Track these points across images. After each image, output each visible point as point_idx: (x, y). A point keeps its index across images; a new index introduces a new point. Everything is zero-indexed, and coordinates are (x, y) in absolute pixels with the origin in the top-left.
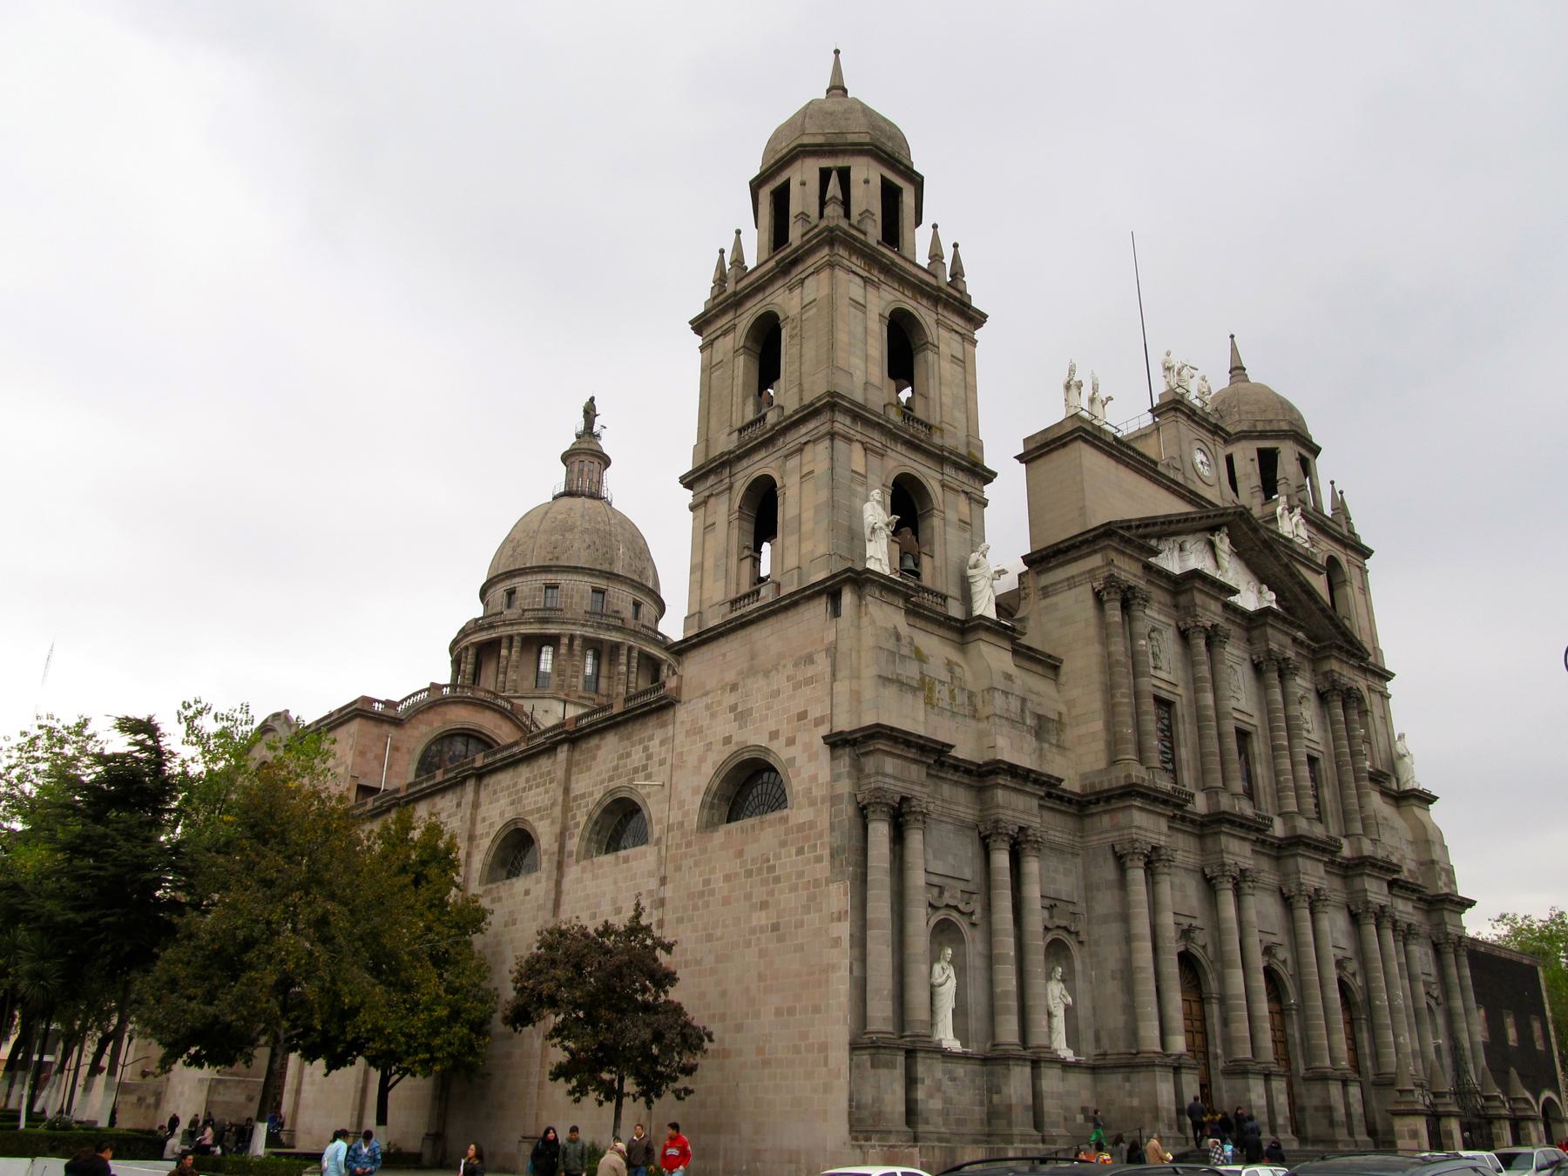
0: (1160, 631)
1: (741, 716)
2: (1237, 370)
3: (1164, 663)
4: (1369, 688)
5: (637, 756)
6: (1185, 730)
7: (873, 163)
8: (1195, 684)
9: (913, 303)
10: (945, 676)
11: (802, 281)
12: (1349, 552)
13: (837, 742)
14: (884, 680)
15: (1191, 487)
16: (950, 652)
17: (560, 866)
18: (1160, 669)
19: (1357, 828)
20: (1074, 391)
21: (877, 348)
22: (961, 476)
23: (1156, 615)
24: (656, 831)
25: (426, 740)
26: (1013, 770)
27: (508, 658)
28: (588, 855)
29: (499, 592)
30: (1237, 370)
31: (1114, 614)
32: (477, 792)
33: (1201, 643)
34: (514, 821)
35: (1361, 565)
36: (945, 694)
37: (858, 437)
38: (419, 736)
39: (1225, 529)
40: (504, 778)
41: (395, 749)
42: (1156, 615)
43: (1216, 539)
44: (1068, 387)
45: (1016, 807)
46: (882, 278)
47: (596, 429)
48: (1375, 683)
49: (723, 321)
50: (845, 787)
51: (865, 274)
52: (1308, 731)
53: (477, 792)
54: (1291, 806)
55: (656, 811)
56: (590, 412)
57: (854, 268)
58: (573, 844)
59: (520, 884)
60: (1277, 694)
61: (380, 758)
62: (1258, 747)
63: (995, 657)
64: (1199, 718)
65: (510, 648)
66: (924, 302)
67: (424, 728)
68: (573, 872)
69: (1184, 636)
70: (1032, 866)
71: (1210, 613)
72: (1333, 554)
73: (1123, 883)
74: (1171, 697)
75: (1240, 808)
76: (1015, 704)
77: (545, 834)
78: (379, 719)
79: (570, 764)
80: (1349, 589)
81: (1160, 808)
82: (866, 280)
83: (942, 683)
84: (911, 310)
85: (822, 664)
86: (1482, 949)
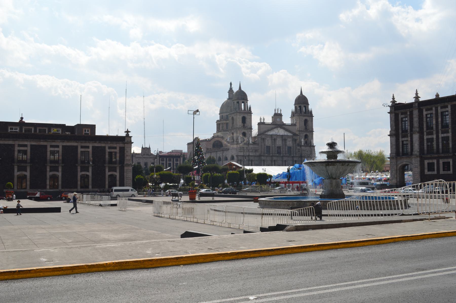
1: (232, 152)
2: (301, 92)
4: (309, 134)
5: (227, 154)
6: (271, 148)
7: (241, 101)
8: (272, 144)
11: (234, 116)
13: (236, 156)
14: (239, 151)
15: (276, 124)
16: (247, 146)
17: (223, 161)
19: (294, 153)
21: (241, 121)
23: (268, 139)
24: (228, 160)
25: (213, 143)
26: (250, 156)
27: (222, 126)
28: (224, 161)
29: (221, 115)
30: (301, 92)
31: (262, 141)
32: (217, 153)
33: (273, 141)
34: (219, 156)
38: (212, 142)
40: (218, 152)
41: (210, 144)
42: (268, 139)
44: (260, 119)
45: (251, 158)
47: (232, 88)
48: (311, 133)
49: (230, 115)
50: (237, 159)
53: (217, 153)
54: (284, 153)
55: (228, 158)
56: (231, 84)
58: (223, 159)
59: (220, 162)
60: (284, 143)
61: (208, 145)
62: (281, 148)
63: (251, 146)
64: (272, 147)
65: (222, 124)
66: (246, 114)
67: (212, 141)
68: (224, 161)
69: (272, 140)
70: (253, 162)
71: (275, 137)
73: (261, 163)
76: (252, 150)
77: (222, 158)
78: (208, 141)
79: (223, 153)
80: (308, 122)
82: (239, 115)
84: (244, 116)
85: (236, 150)
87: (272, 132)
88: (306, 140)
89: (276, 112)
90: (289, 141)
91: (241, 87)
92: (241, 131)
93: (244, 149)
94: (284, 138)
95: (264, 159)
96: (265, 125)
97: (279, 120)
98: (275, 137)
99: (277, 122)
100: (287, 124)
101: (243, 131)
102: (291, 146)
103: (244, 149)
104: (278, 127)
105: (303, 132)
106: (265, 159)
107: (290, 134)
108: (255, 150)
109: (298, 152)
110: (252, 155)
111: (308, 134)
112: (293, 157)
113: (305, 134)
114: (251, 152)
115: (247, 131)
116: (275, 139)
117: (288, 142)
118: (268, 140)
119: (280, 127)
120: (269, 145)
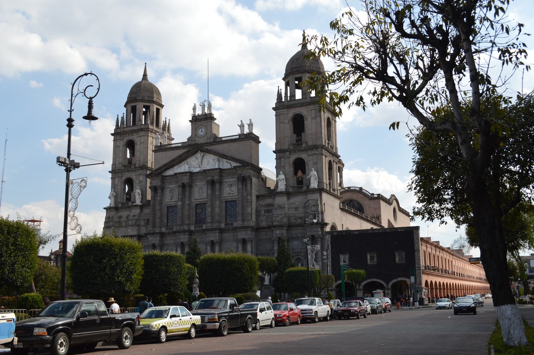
0: (174, 189)
3: (175, 197)
4: (308, 155)
9: (132, 136)
10: (125, 219)
12: (308, 107)
15: (194, 143)
18: (173, 199)
20: (157, 139)
22: (140, 171)
23: (173, 186)
35: (315, 108)
36: (124, 223)
37: (116, 176)
39: (199, 151)
42: (173, 186)
43: (196, 155)
46: (124, 136)
51: (120, 138)
52: (233, 194)
57: (117, 139)
71: (185, 180)
72: (297, 113)
74: (176, 205)
75: (183, 228)
76: (134, 221)
81: (155, 235)
83: (124, 221)
84: (130, 139)
86: (357, 233)
87: (183, 166)
88: (300, 173)
89: (199, 112)
90: (231, 186)
91: (148, 74)
92: (122, 177)
93: (121, 220)
94: (209, 178)
95: (153, 242)
96: (165, 152)
97: (200, 130)
98: (185, 178)
99: (197, 139)
100: (226, 139)
101: (127, 175)
102: (234, 198)
103: (121, 220)
104: (197, 152)
105: (288, 153)
106: (157, 242)
107: (226, 165)
108: (146, 221)
109: (267, 214)
110: (135, 233)
111: (303, 156)
112: (235, 229)
113: (293, 157)
114: (132, 226)
115: (136, 175)
116: (183, 186)
117: (228, 189)
118: (172, 190)
119: (201, 151)
120: (173, 204)
